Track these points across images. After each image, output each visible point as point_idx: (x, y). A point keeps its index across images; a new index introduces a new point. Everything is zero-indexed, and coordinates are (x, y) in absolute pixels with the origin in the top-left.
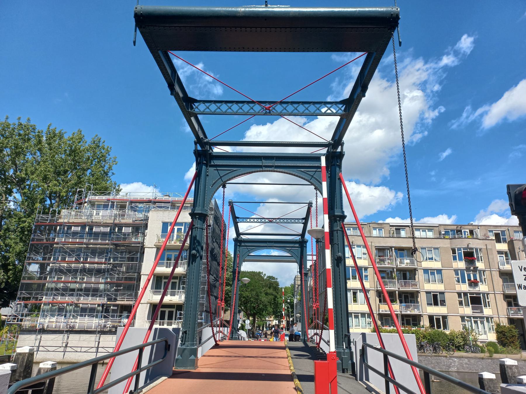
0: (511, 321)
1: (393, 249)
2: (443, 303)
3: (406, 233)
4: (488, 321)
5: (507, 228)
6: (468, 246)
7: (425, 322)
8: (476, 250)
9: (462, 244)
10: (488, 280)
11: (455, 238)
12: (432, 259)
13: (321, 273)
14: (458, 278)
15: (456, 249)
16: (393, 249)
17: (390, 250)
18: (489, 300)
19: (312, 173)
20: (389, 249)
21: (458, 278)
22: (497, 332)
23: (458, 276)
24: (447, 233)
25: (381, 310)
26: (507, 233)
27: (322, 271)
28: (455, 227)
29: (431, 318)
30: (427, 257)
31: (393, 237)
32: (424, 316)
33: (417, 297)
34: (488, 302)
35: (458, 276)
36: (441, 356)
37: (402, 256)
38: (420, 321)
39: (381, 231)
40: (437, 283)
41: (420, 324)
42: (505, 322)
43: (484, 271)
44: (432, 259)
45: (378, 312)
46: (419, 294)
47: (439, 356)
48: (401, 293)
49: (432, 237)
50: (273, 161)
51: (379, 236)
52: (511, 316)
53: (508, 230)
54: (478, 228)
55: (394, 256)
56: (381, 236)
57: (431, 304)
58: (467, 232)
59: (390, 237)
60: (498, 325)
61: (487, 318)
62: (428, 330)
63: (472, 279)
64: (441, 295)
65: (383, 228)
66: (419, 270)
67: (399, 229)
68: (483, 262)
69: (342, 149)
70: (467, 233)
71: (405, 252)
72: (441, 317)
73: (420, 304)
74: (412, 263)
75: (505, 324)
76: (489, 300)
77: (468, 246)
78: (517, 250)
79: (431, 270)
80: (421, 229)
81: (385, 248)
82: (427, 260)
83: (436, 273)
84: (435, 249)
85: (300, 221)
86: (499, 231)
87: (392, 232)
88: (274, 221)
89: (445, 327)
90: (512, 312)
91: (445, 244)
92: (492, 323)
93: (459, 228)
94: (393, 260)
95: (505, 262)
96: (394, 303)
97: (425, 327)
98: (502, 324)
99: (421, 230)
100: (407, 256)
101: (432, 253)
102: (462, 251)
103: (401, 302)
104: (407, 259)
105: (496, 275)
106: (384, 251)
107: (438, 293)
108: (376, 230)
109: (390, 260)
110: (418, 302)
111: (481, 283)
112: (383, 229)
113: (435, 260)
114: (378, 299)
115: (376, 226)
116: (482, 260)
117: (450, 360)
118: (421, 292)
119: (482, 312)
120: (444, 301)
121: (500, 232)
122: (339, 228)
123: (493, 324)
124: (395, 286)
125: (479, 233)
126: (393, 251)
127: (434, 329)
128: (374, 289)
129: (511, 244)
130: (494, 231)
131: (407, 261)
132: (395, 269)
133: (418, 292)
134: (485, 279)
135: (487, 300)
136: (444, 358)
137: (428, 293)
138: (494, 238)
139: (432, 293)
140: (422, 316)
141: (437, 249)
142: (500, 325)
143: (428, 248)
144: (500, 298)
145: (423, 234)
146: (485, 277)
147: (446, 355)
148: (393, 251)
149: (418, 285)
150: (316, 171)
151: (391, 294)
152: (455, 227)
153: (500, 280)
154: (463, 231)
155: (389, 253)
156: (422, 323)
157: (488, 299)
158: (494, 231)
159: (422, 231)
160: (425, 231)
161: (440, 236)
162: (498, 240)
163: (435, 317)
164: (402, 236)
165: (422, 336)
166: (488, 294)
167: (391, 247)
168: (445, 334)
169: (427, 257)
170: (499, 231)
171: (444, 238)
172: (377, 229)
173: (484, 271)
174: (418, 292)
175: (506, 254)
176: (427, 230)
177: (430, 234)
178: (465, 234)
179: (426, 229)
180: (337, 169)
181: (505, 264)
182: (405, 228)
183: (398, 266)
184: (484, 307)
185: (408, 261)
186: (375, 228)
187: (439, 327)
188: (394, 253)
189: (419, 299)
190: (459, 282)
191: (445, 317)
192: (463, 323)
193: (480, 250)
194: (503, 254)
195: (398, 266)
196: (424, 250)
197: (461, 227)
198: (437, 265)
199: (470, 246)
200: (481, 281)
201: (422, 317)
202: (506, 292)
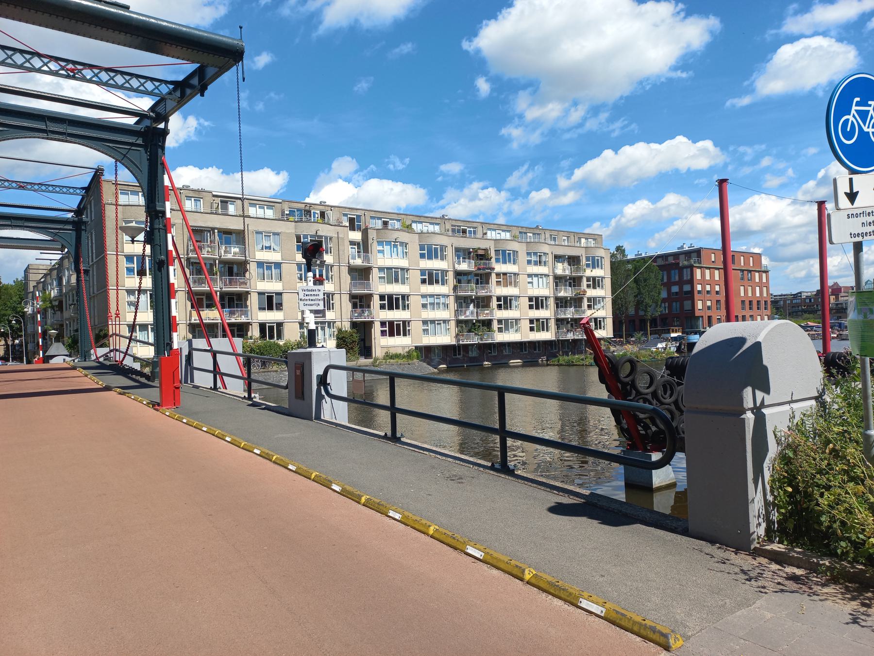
0: (354, 325)
1: (216, 231)
2: (279, 307)
3: (236, 209)
4: (329, 327)
5: (363, 212)
6: (316, 232)
7: (255, 332)
8: (326, 238)
9: (309, 230)
10: (336, 278)
11: (301, 221)
12: (270, 248)
13: (93, 265)
14: (301, 275)
15: (302, 236)
16: (216, 231)
17: (212, 232)
18: (334, 302)
19: (124, 152)
20: (210, 231)
21: (301, 275)
22: (338, 338)
23: (301, 272)
24: (292, 213)
25: (193, 318)
26: (363, 218)
27: (95, 261)
28: (303, 206)
29: (262, 326)
30: (263, 246)
31: (216, 214)
32: (253, 324)
33: (246, 299)
34: (333, 304)
35: (301, 272)
36: (270, 372)
37: (228, 242)
38: (247, 330)
39: (199, 202)
40: (274, 281)
41: (247, 335)
42: (347, 326)
43: (332, 266)
44: (270, 248)
45: (189, 322)
46: (249, 295)
47: (268, 371)
48: (223, 295)
49: (272, 217)
50: (65, 126)
51: (196, 210)
52: (354, 320)
53: (365, 215)
54: (331, 210)
55: (216, 242)
56: (199, 210)
57: (264, 309)
58: (318, 214)
59: (212, 213)
60: (340, 330)
61: (329, 323)
62: (258, 342)
63: (318, 276)
64: (279, 297)
65: (202, 198)
66: (251, 263)
67: (227, 202)
68: (332, 254)
69: (166, 125)
70: (317, 216)
71: (233, 237)
72: (275, 325)
73: (249, 308)
74: (244, 252)
75: (347, 329)
76: (334, 302)
77: (316, 232)
78: (370, 241)
79: (267, 263)
80: (258, 204)
81: (203, 229)
82: (262, 249)
83: (273, 267)
84: (274, 234)
85: (78, 191)
86: (354, 215)
87: (215, 206)
88: (29, 187)
89: (279, 336)
90: (356, 315)
91: (288, 228)
92: (333, 328)
93: (307, 208)
94: (214, 248)
95: (357, 255)
96: (213, 309)
97: (253, 338)
98: (343, 329)
99: (258, 206)
100: (235, 243)
101: (270, 240)
102: (309, 239)
103: (223, 307)
104: (235, 247)
105: (345, 270)
106: (202, 233)
107: (274, 295)
108: (191, 200)
109: (211, 247)
110: (246, 306)
111: (327, 281)
112: (201, 200)
113: (274, 250)
114: (189, 304)
115: (191, 194)
116: (331, 253)
117: (281, 374)
118: (252, 293)
119: (324, 316)
120: (281, 304)
121: (355, 217)
122: (161, 226)
123: (335, 330)
124: (218, 286)
125: (332, 216)
126: (216, 234)
127: (265, 340)
128: (184, 289)
129: (365, 233)
130: (350, 214)
131: (235, 250)
132: (217, 261)
133: (248, 293)
134: (332, 275)
135: (331, 302)
136: (274, 374)
137: (260, 294)
138: (347, 224)
139: (266, 294)
140: (251, 325)
141: (278, 234)
142: (341, 331)
143: (265, 232)
144: (346, 298)
145: (260, 213)
146: (333, 274)
147: (277, 369)
148: (216, 234)
149: (248, 284)
150: (130, 149)
151: (209, 296)
152: (303, 206)
153: (349, 277)
154: (312, 211)
155: (209, 237)
156: (250, 334)
157: (333, 300)
158: (350, 214)
159: (259, 207)
160: (264, 208)
161: (283, 217)
162: (352, 226)
163: (267, 325)
164: (230, 213)
165: (248, 349)
166: (333, 294)
167: (213, 229)
168: (278, 345)
169: (263, 246)
170: (354, 215)
171: (288, 220)
172: (193, 199)
173: (332, 266)
174: (248, 293)
175: (359, 244)
176: (265, 207)
177: (269, 213)
178: (314, 217)
179: (265, 205)
180: (160, 150)
181: (357, 257)
182: (235, 201)
183: (222, 257)
184: (327, 310)
185: (237, 250)
186: (189, 198)
187: (272, 337)
188: (217, 238)
189: (248, 303)
190: (301, 279)
191: (280, 325)
192: (302, 330)
193: (331, 239)
194: (356, 245)
195: (222, 257)
196: (261, 235)
197: (310, 206)
198: (274, 257)
199: (319, 233)
200: (327, 278)
201: (250, 326)
202: (353, 292)
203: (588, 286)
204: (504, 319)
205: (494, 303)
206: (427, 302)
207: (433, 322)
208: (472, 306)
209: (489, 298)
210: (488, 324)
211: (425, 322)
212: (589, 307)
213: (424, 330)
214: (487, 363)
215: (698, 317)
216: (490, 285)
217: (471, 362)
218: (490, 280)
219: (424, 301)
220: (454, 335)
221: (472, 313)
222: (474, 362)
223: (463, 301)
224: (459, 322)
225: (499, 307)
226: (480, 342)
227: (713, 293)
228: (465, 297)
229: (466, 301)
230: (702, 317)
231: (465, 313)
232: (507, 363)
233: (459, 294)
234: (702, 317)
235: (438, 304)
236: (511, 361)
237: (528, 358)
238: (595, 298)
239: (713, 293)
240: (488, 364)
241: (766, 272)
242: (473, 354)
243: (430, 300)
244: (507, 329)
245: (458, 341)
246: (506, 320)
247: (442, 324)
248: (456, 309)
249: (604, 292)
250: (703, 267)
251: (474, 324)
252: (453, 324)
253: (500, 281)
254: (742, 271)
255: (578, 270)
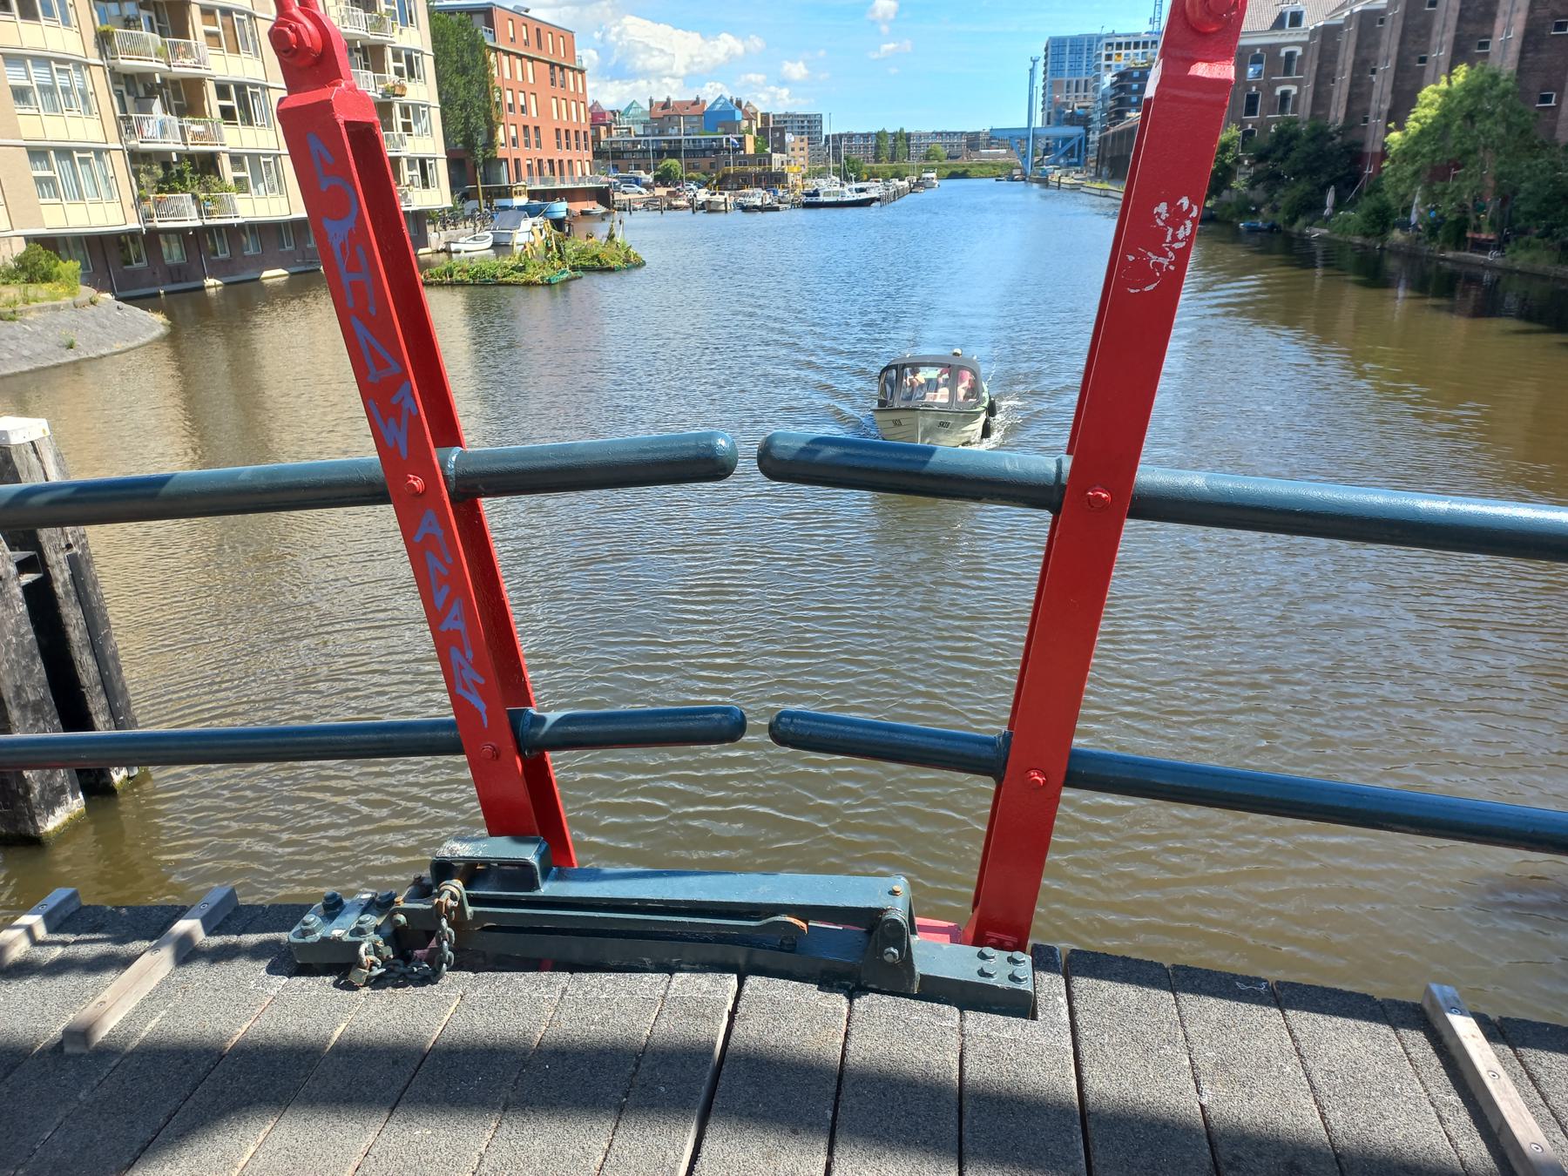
203: (399, 72)
204: (247, 154)
205: (213, 103)
206: (27, 83)
207: (65, 153)
208: (157, 105)
209: (195, 85)
210: (206, 164)
211: (37, 154)
212: (407, 127)
213: (39, 181)
214: (210, 282)
215: (500, 161)
216: (192, 41)
217: (173, 282)
218: (190, 26)
219: (16, 76)
220: (128, 199)
221: (163, 130)
222: (180, 281)
223: (123, 88)
224: (138, 158)
225: (227, 113)
226: (208, 222)
227: (518, 109)
228: (125, 76)
229: (132, 89)
230: (506, 160)
231: (141, 130)
232: (258, 279)
233: (122, 62)
234: (506, 160)
235: (66, 91)
236: (266, 274)
237: (299, 265)
238: (415, 106)
239: (518, 109)
240: (215, 286)
241: (582, 71)
242: (173, 253)
243: (38, 76)
244: (257, 178)
245: (148, 217)
246: (254, 158)
247: (94, 161)
248: (118, 114)
249: (423, 91)
250: (499, 50)
251: (166, 165)
252: (119, 165)
253: (216, 35)
254: (552, 65)
255: (378, 26)
